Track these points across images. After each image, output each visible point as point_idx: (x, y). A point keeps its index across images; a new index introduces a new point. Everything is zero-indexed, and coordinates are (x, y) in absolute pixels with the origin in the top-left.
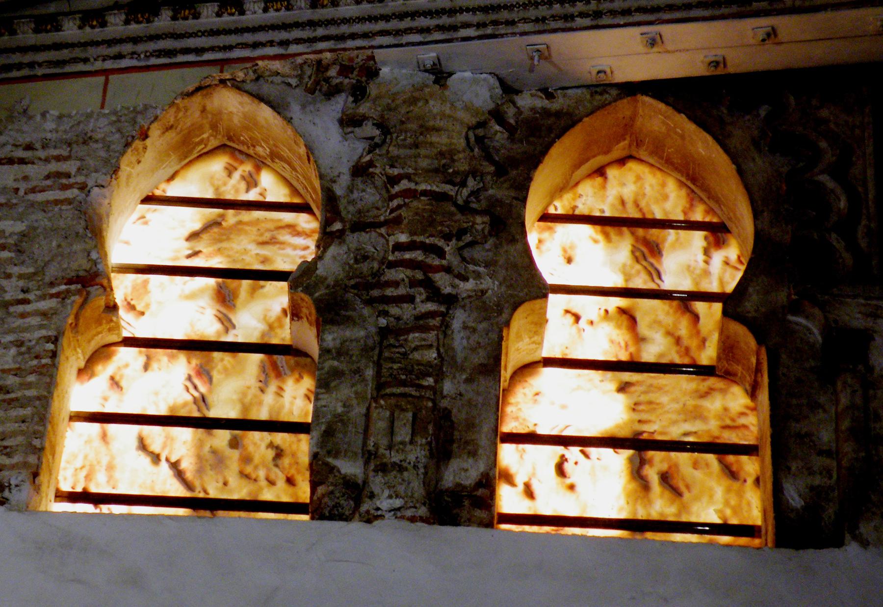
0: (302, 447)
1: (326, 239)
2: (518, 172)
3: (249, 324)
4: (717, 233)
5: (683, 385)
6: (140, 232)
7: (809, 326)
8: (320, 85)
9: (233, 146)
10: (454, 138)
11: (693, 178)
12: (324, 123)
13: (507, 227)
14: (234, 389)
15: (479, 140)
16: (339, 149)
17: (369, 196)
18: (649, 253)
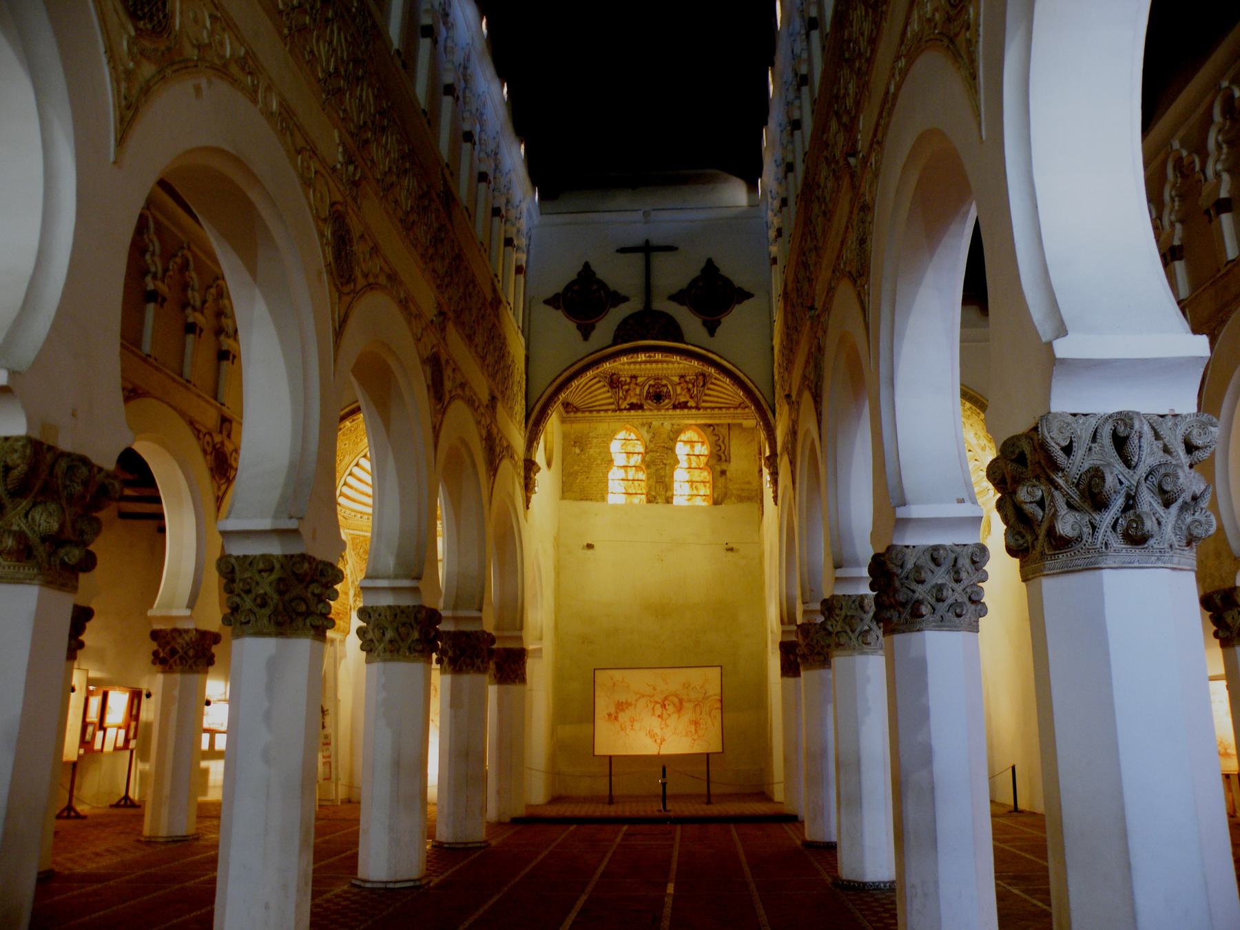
0: (643, 484)
1: (646, 453)
2: (674, 440)
3: (632, 463)
4: (703, 443)
5: (698, 471)
6: (615, 447)
7: (718, 468)
8: (643, 425)
9: (627, 429)
10: (665, 436)
11: (699, 435)
12: (644, 431)
13: (672, 449)
14: (632, 474)
15: (668, 436)
16: (647, 437)
17: (652, 446)
18: (692, 447)
